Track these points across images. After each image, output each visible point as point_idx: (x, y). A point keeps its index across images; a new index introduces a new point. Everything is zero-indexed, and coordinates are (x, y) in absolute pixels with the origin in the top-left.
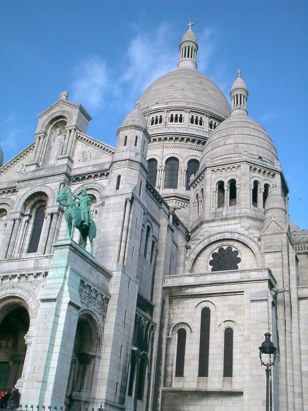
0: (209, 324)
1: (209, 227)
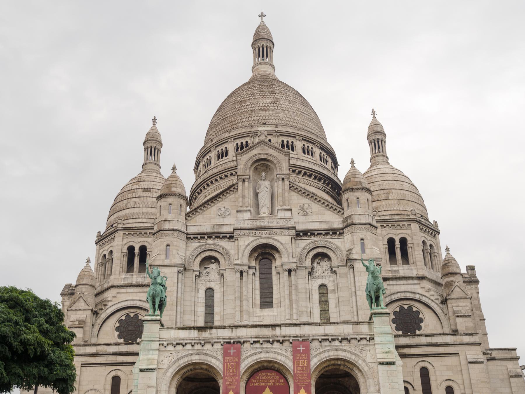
0: (422, 383)
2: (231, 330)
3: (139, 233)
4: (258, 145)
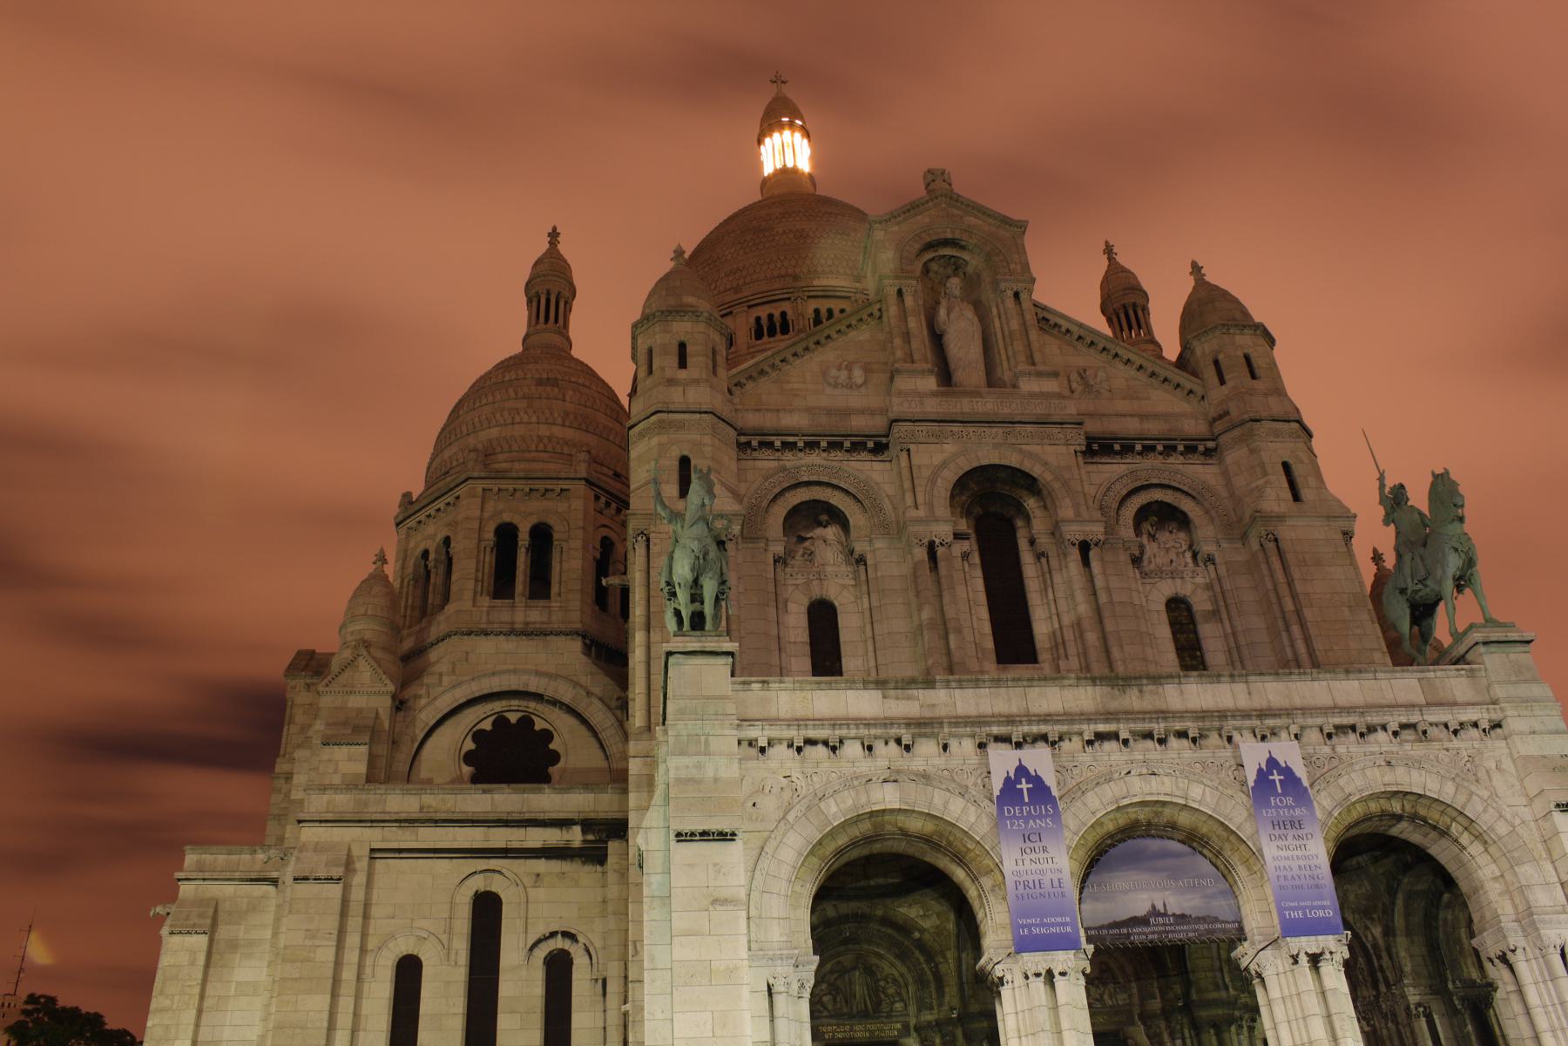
3: (531, 490)
4: (931, 204)
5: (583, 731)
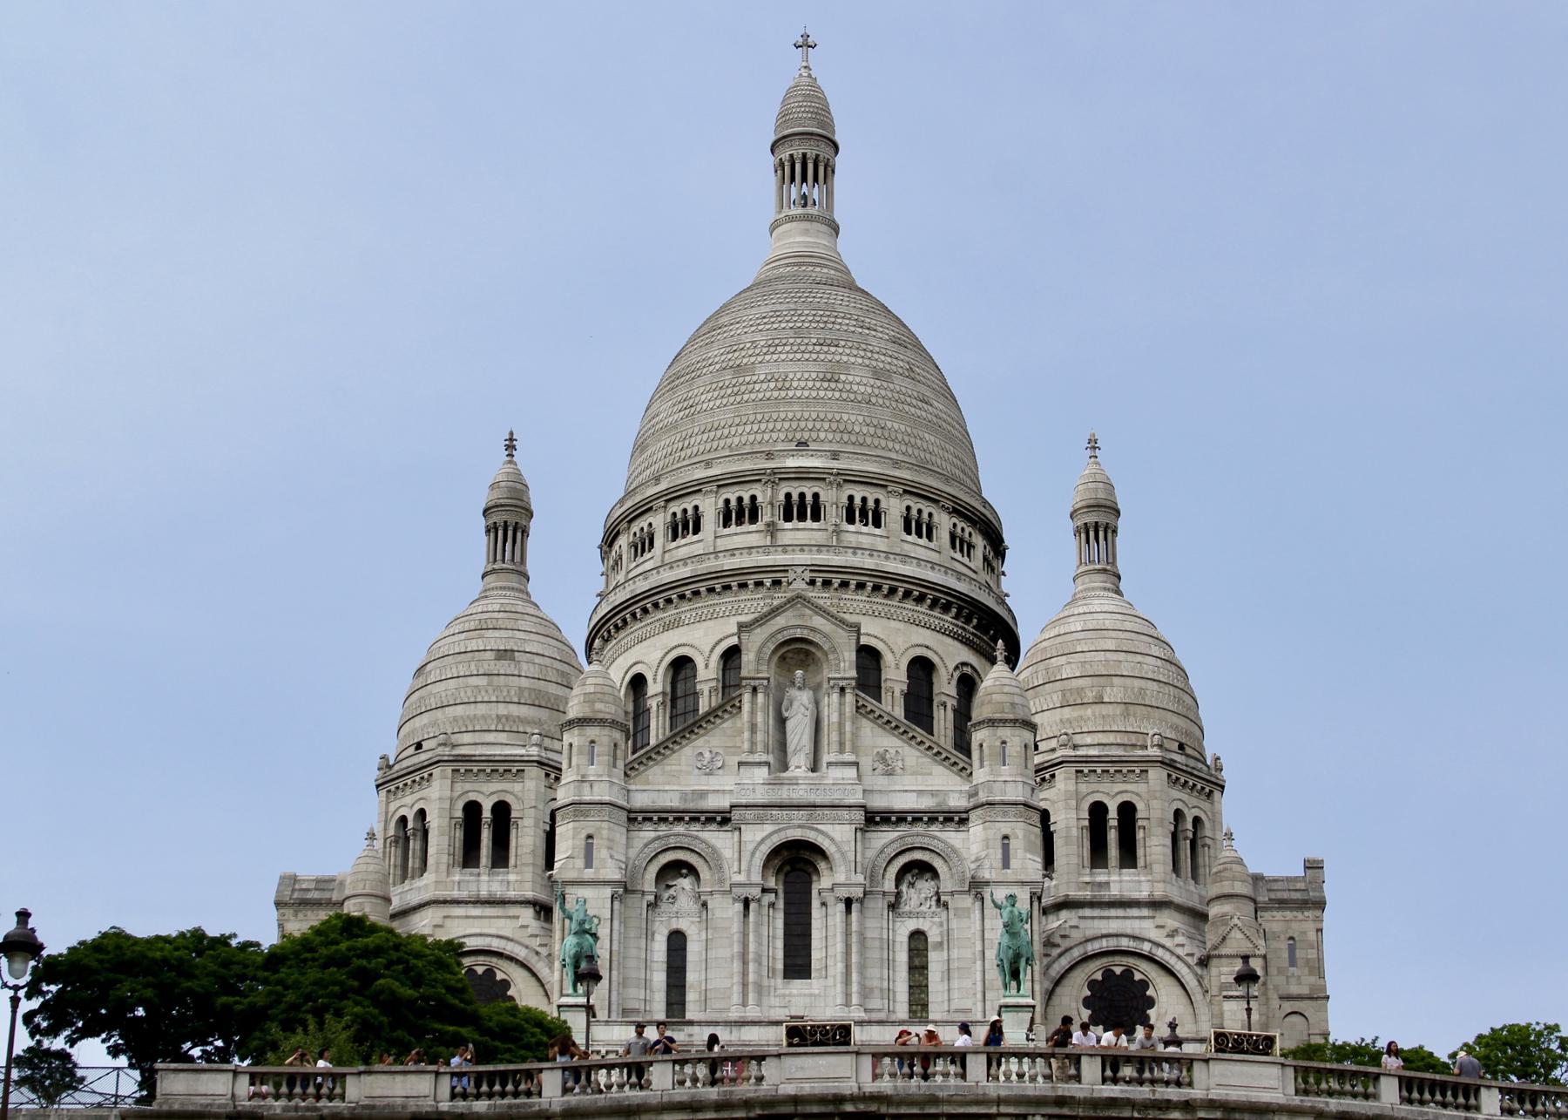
1: (1080, 917)
2: (728, 1028)
3: (492, 771)
5: (533, 981)
